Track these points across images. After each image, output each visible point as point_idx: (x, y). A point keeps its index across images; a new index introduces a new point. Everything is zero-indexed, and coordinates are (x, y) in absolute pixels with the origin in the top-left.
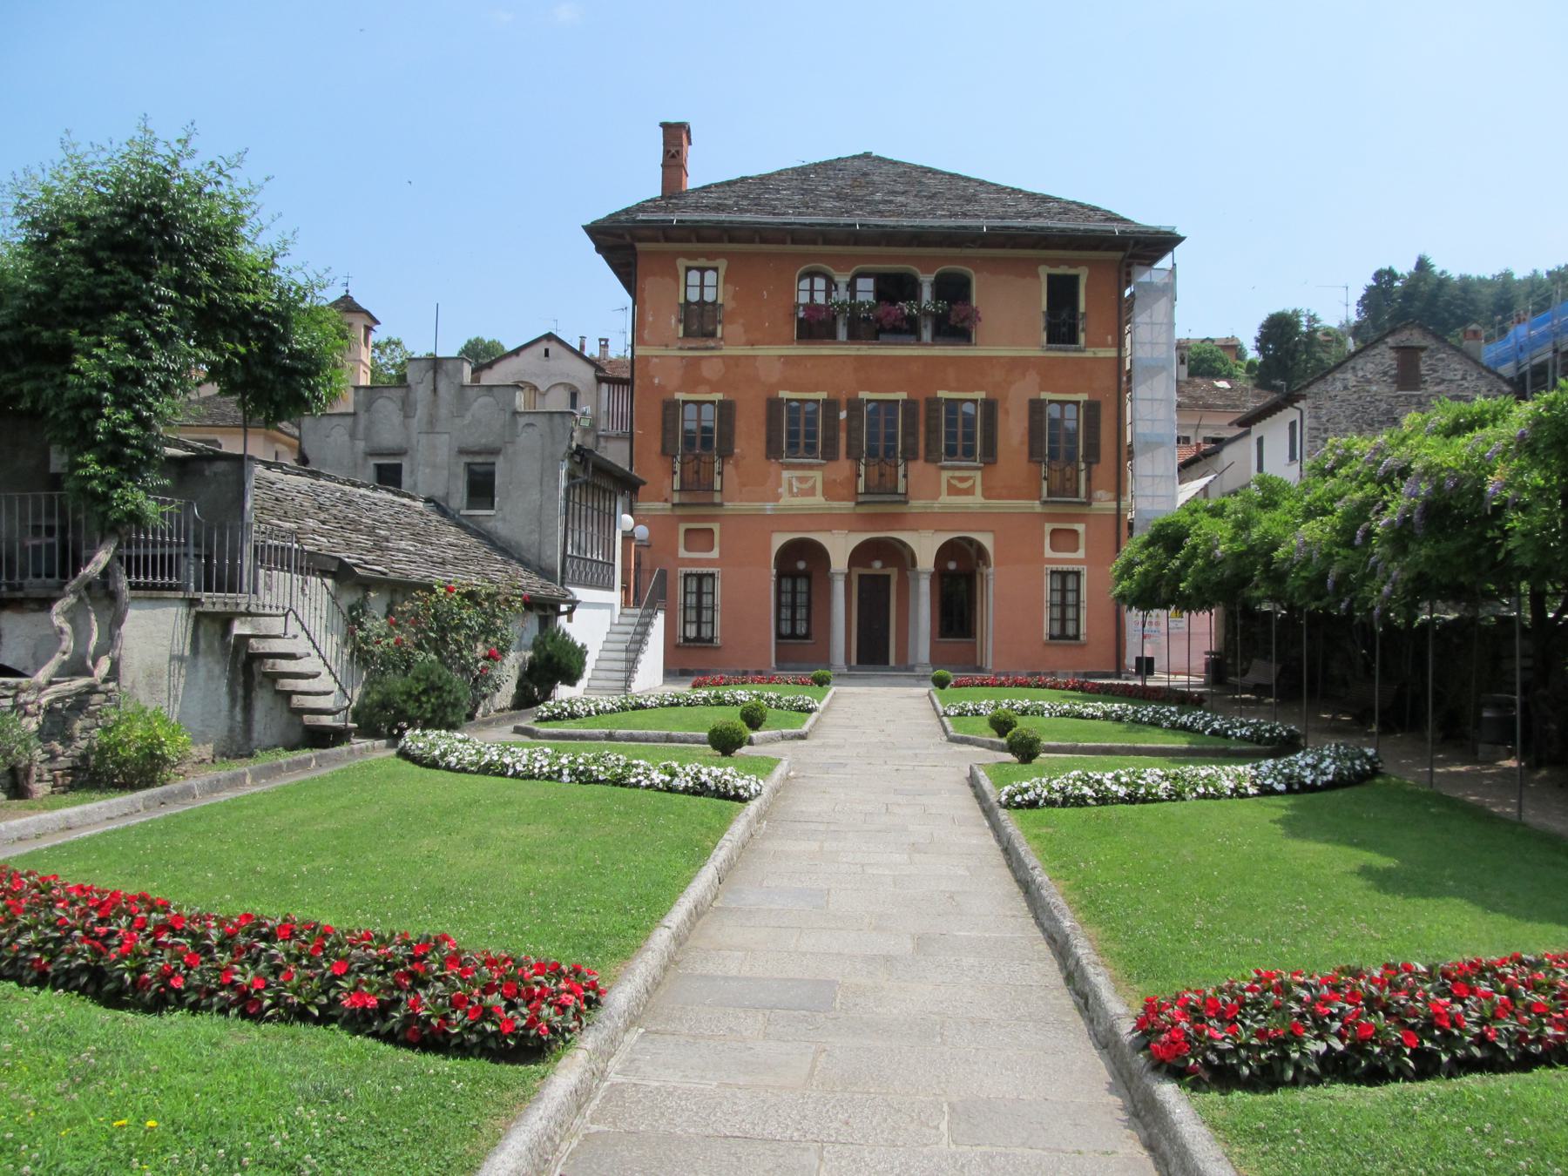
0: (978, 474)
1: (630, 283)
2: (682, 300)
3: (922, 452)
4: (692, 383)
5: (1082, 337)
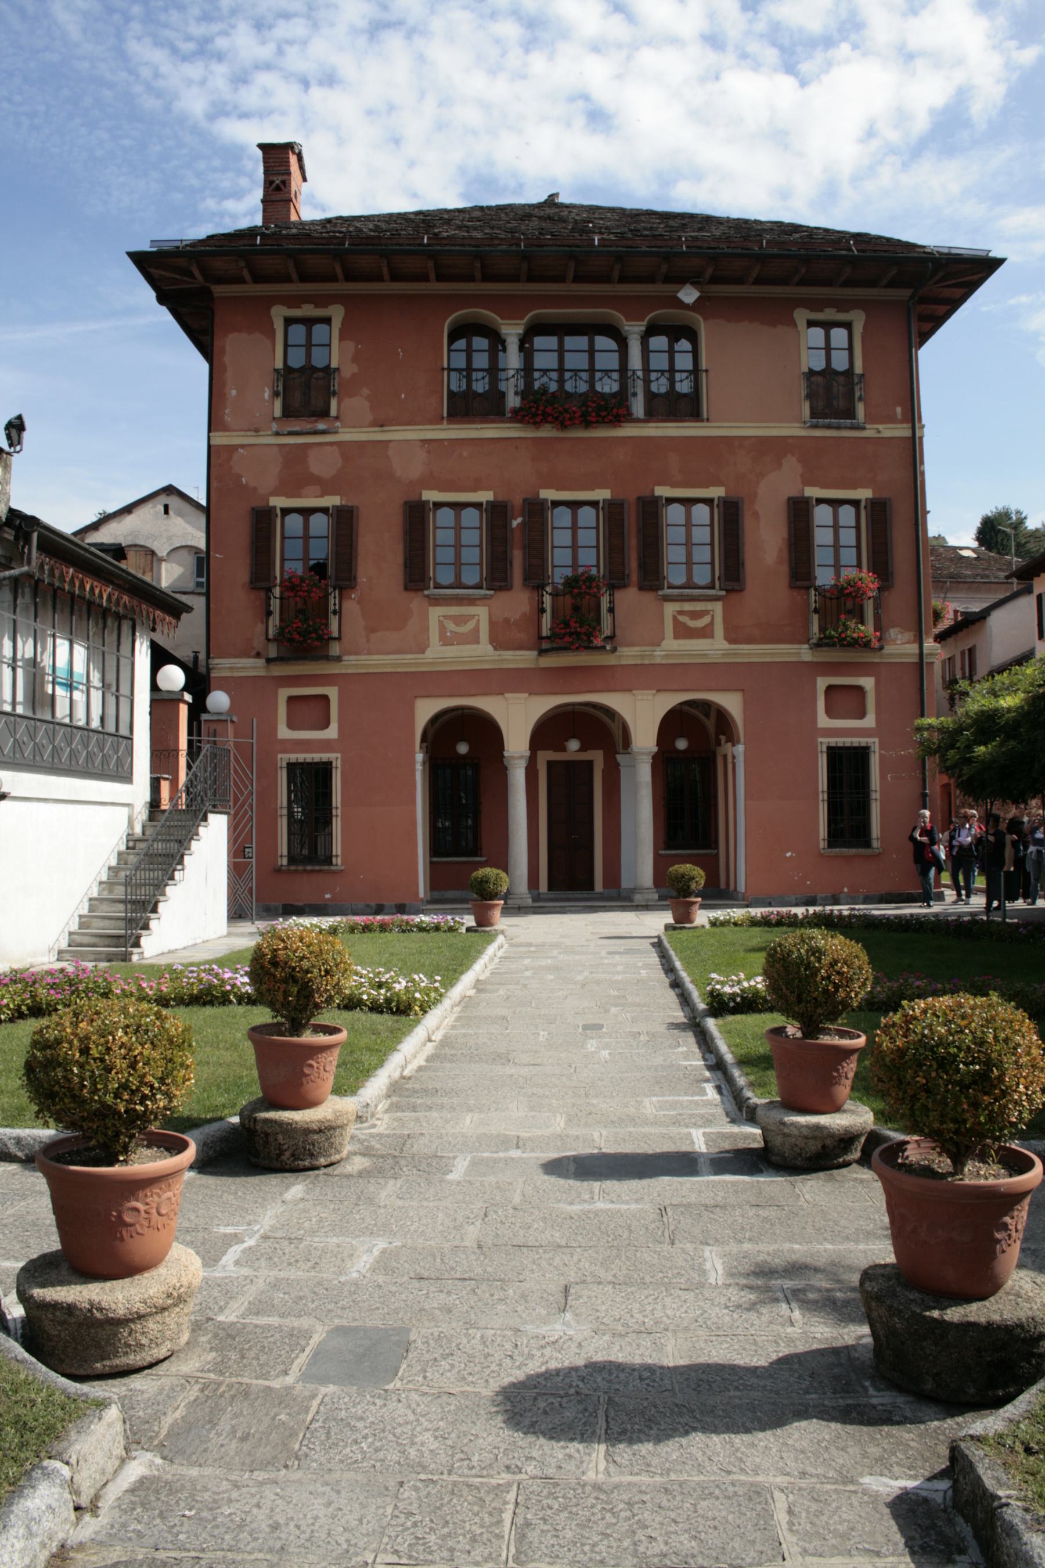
0: (718, 608)
1: (206, 350)
2: (279, 364)
3: (634, 577)
4: (291, 485)
5: (860, 409)
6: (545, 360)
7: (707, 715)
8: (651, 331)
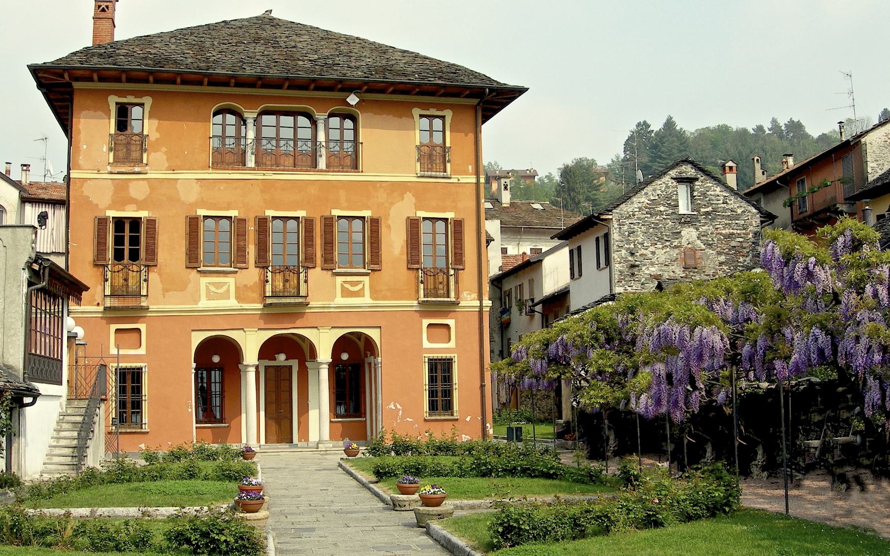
0: (366, 279)
6: (268, 132)
7: (359, 339)
8: (331, 115)
